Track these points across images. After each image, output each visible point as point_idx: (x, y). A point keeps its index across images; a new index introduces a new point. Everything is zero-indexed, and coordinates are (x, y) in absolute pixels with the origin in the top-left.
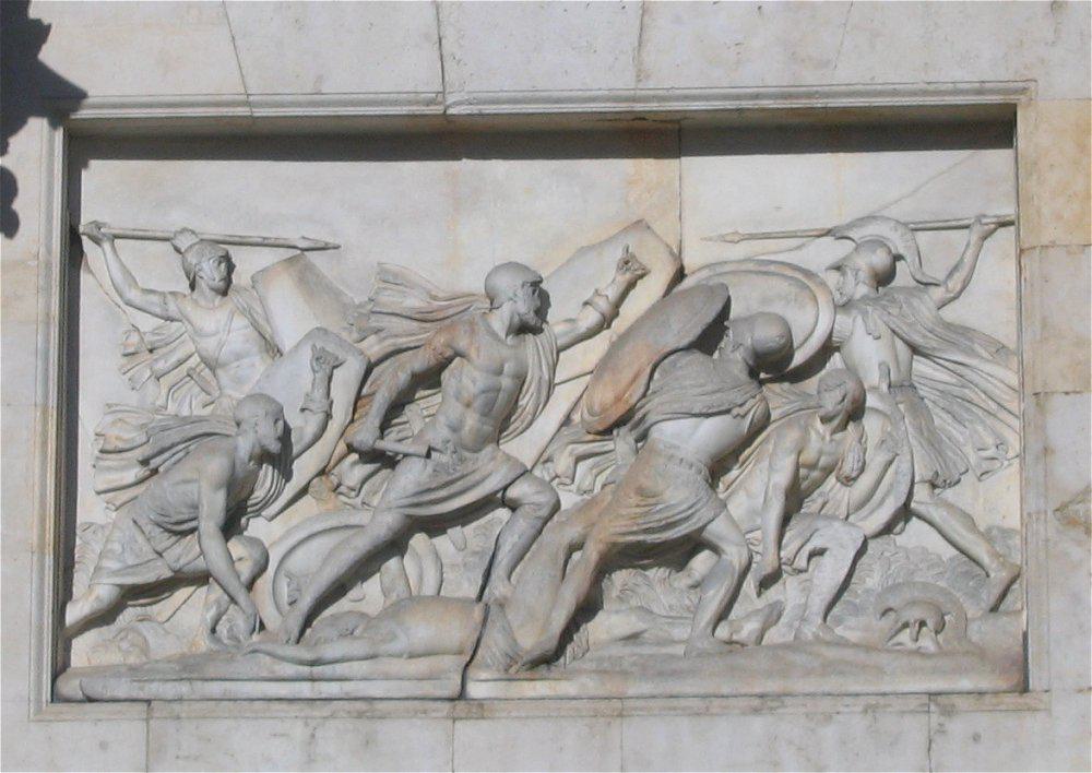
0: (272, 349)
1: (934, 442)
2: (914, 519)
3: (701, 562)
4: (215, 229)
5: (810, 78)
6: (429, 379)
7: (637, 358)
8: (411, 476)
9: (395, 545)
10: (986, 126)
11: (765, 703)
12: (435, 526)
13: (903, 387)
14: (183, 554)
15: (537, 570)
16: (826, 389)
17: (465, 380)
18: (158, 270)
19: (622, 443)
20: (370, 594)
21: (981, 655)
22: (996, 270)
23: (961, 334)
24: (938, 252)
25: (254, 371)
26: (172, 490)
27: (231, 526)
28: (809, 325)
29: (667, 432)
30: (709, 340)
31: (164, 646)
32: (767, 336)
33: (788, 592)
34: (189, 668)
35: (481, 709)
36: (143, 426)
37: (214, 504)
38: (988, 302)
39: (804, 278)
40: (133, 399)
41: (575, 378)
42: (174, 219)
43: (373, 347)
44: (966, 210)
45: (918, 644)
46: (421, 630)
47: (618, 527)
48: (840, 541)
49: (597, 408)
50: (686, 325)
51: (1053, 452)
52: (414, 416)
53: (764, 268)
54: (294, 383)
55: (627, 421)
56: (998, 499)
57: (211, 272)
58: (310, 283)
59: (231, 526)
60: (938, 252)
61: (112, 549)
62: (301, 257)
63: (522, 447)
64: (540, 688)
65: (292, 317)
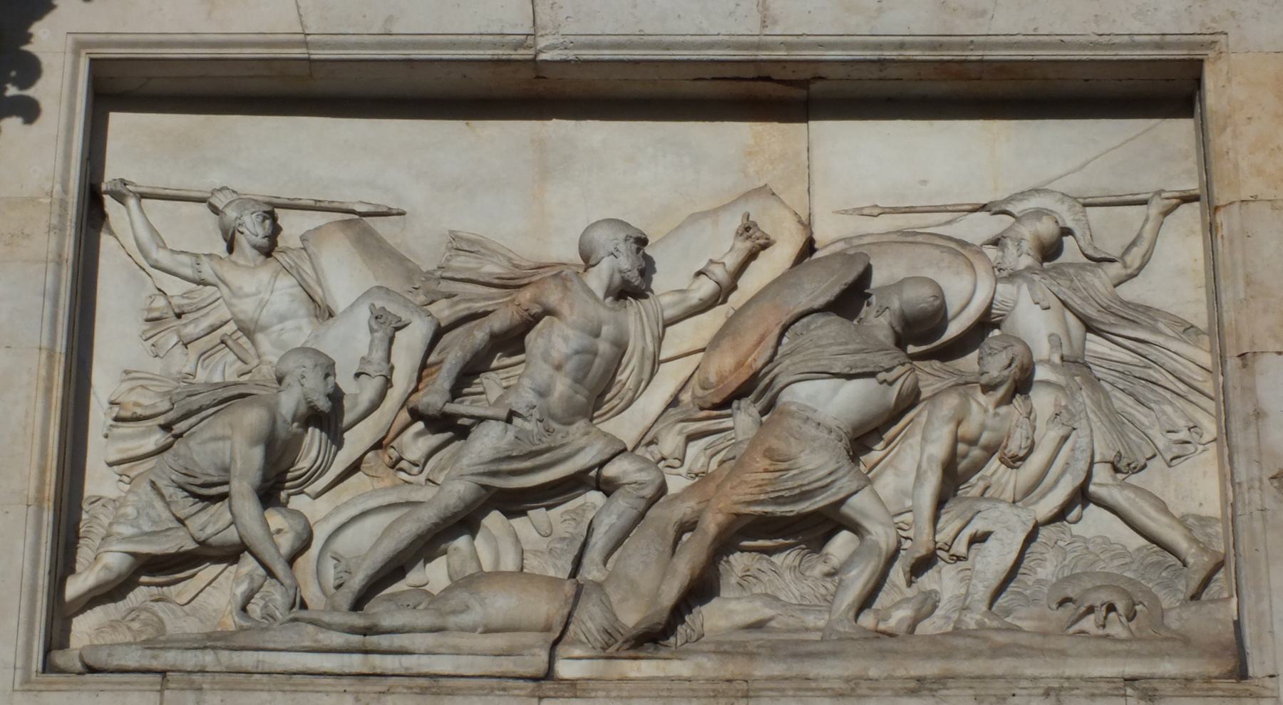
0: (323, 312)
2: (1092, 506)
3: (841, 544)
5: (963, 26)
6: (511, 341)
8: (488, 442)
9: (464, 522)
12: (514, 503)
13: (1075, 363)
14: (212, 524)
16: (992, 361)
17: (555, 342)
18: (192, 231)
19: (744, 418)
20: (434, 574)
21: (1184, 643)
22: (1181, 246)
23: (1142, 314)
25: (300, 330)
27: (269, 494)
28: (965, 295)
29: (802, 394)
30: (850, 300)
32: (919, 298)
36: (165, 394)
38: (1173, 274)
39: (960, 249)
40: (156, 367)
41: (687, 353)
43: (444, 311)
44: (1144, 184)
45: (1108, 630)
47: (742, 495)
49: (713, 378)
50: (821, 287)
51: (1265, 415)
52: (491, 384)
53: (907, 238)
54: (350, 342)
55: (753, 388)
56: (1196, 487)
57: (253, 229)
59: (269, 494)
61: (125, 512)
62: (360, 223)
63: (626, 427)
64: (645, 668)
65: (345, 276)
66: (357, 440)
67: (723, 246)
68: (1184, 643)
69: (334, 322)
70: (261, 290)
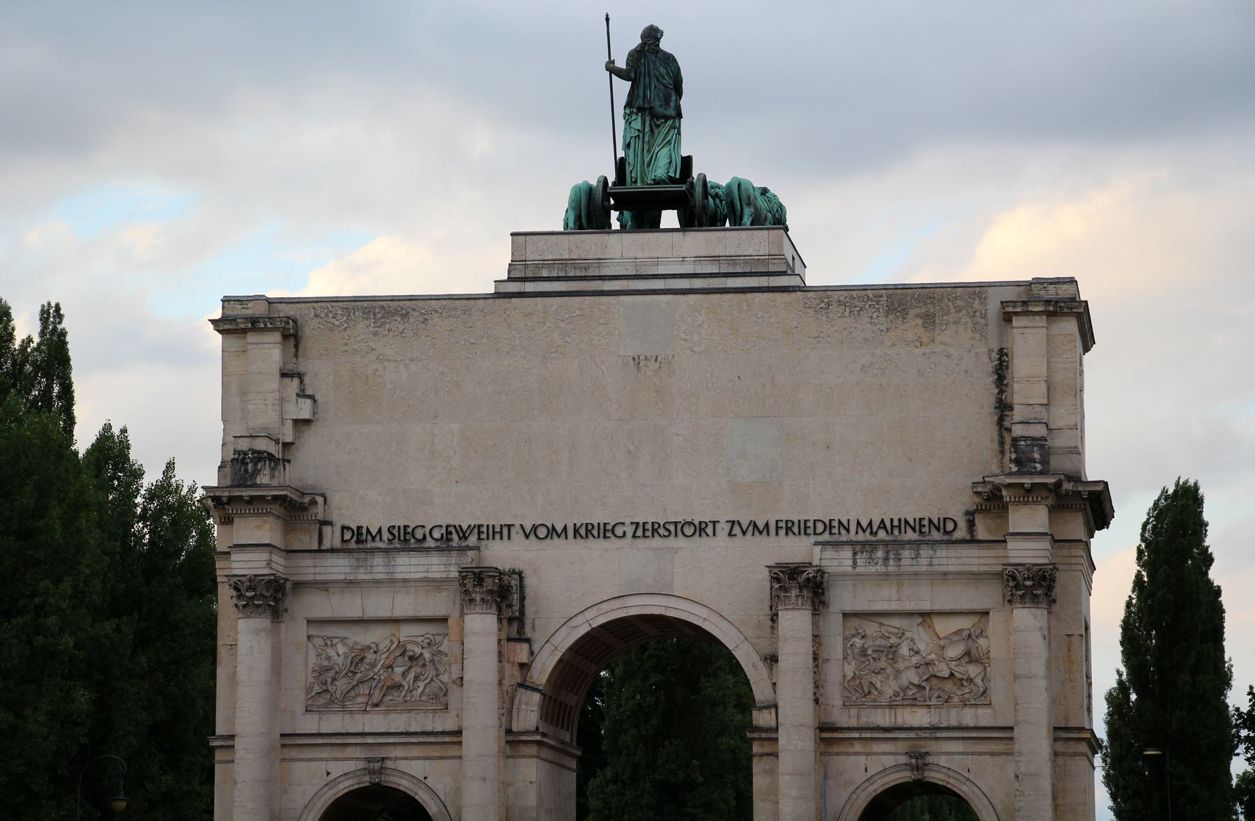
1: (436, 669)
7: (392, 657)
8: (358, 676)
10: (444, 620)
15: (377, 691)
20: (352, 694)
24: (438, 639)
26: (322, 678)
28: (418, 650)
30: (403, 654)
34: (325, 706)
39: (417, 643)
46: (360, 700)
48: (422, 685)
50: (398, 652)
53: (411, 642)
54: (340, 661)
55: (391, 667)
58: (344, 644)
60: (438, 639)
62: (343, 640)
63: (376, 670)
65: (341, 649)
67: (387, 642)
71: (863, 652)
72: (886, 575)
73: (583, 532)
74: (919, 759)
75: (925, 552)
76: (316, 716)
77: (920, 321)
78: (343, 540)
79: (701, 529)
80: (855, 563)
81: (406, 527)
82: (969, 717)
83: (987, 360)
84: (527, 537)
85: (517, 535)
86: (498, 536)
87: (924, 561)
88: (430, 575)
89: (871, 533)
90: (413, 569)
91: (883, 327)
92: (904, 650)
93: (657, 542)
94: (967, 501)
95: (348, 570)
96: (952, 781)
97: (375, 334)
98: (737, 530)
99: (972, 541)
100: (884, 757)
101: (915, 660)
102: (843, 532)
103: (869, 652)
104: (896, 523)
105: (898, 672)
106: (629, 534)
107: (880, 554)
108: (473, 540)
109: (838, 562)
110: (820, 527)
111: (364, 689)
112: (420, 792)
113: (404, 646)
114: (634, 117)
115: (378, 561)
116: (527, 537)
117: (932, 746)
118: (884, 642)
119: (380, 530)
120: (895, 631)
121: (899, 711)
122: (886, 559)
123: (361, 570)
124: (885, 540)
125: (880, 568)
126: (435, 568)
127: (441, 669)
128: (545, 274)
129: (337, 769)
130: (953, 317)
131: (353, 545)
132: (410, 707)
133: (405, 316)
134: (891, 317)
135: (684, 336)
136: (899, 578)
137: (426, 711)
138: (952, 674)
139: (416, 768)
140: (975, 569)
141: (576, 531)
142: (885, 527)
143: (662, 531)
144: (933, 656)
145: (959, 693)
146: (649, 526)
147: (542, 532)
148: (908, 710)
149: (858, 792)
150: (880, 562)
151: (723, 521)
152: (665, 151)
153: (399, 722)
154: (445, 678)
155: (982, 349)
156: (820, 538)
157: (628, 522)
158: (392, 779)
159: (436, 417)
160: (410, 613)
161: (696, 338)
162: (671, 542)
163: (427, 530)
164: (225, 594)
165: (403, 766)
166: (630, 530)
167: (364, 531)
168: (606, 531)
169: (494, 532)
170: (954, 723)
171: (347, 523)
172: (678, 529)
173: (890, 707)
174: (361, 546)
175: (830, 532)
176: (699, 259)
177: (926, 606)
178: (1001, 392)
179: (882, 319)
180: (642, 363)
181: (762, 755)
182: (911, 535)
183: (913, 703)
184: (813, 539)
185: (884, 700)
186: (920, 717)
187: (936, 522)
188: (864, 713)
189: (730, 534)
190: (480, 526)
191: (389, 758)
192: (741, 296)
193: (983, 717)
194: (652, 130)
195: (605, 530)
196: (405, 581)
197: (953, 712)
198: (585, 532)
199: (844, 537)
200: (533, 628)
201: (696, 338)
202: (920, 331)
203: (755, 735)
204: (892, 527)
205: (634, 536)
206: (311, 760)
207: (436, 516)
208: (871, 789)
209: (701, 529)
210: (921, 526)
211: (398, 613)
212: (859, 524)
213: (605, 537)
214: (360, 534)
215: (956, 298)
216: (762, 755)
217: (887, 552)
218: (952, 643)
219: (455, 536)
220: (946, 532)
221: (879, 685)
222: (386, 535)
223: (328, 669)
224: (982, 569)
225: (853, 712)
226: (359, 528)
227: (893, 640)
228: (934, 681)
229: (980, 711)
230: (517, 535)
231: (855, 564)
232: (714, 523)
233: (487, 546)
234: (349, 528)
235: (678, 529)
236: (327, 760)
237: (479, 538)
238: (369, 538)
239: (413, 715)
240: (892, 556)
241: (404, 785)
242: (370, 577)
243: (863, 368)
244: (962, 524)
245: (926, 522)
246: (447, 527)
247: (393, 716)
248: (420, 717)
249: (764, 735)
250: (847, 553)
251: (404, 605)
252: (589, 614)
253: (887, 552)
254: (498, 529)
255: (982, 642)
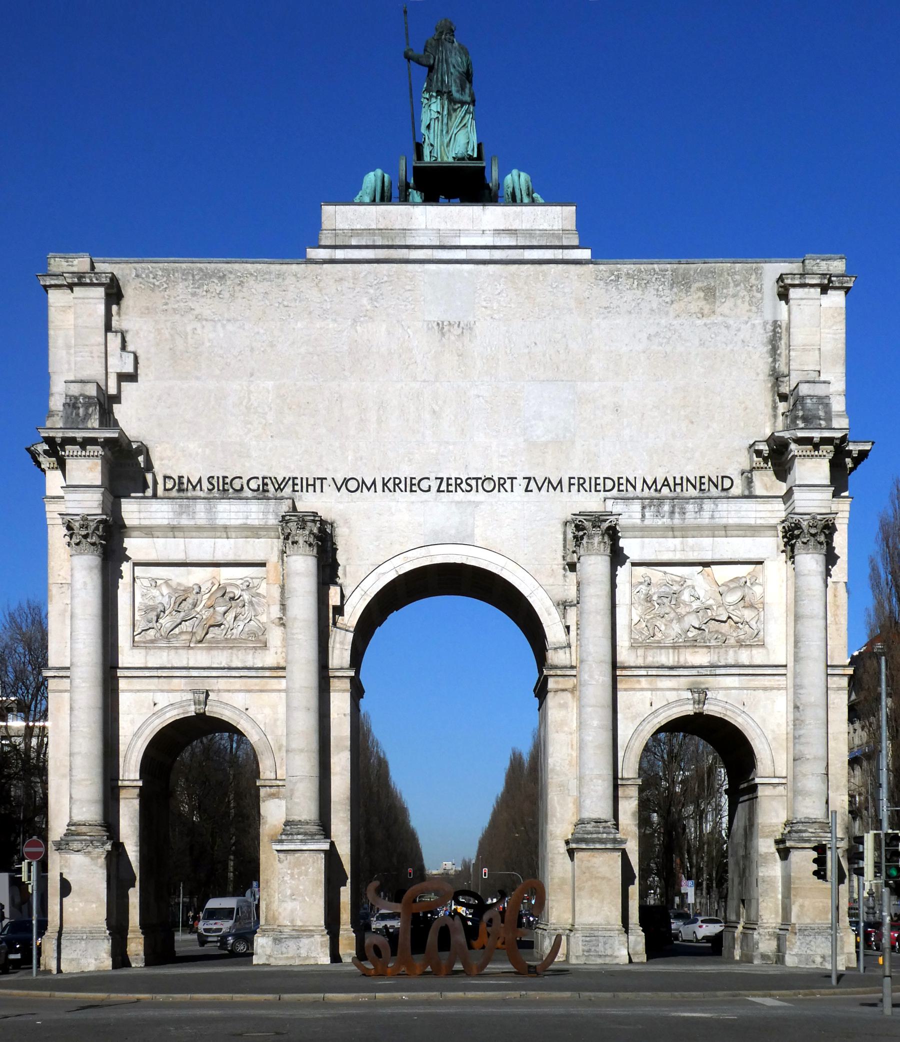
1: (255, 610)
3: (222, 627)
4: (154, 577)
5: (238, 558)
6: (185, 600)
7: (213, 598)
8: (182, 614)
9: (180, 624)
10: (263, 565)
11: (231, 648)
13: (251, 603)
14: (150, 625)
18: (146, 583)
19: (212, 609)
20: (177, 631)
21: (260, 641)
23: (258, 595)
25: (160, 597)
27: (157, 621)
28: (237, 593)
29: (217, 609)
31: (148, 638)
32: (232, 595)
33: (234, 631)
34: (152, 641)
35: (192, 648)
37: (155, 618)
39: (237, 586)
42: (149, 575)
43: (177, 595)
44: (260, 576)
46: (184, 637)
47: (211, 622)
48: (242, 624)
50: (221, 594)
53: (231, 585)
57: (154, 584)
59: (157, 621)
61: (141, 625)
62: (167, 582)
63: (198, 609)
64: (200, 645)
65: (165, 590)
66: (167, 613)
67: (209, 585)
68: (260, 641)
69: (163, 597)
70: (155, 592)
71: (648, 599)
72: (672, 529)
73: (390, 485)
74: (701, 694)
75: (708, 505)
76: (143, 651)
77: (702, 294)
78: (165, 490)
79: (500, 484)
80: (643, 516)
81: (224, 478)
82: (744, 656)
83: (762, 331)
84: (339, 490)
85: (329, 488)
86: (311, 488)
87: (706, 514)
88: (249, 522)
89: (656, 490)
90: (233, 515)
91: (668, 299)
92: (686, 596)
93: (460, 495)
94: (744, 461)
95: (171, 515)
96: (729, 713)
97: (194, 294)
98: (532, 485)
99: (751, 496)
100: (668, 693)
101: (696, 605)
102: (630, 488)
103: (655, 598)
104: (678, 481)
105: (680, 618)
106: (434, 489)
107: (666, 508)
108: (288, 490)
109: (629, 514)
110: (609, 484)
111: (185, 626)
112: (242, 722)
113: (225, 588)
114: (434, 100)
115: (200, 506)
116: (339, 490)
117: (711, 681)
118: (668, 590)
119: (200, 481)
120: (678, 579)
121: (682, 650)
122: (672, 512)
123: (184, 516)
124: (671, 496)
125: (666, 521)
126: (254, 516)
127: (260, 610)
128: (354, 242)
129: (164, 700)
130: (731, 290)
131: (174, 493)
132: (230, 644)
133: (222, 278)
134: (675, 290)
135: (484, 304)
136: (683, 531)
137: (246, 648)
138: (729, 617)
139: (239, 700)
140: (752, 522)
141: (385, 484)
142: (668, 485)
143: (464, 486)
144: (711, 602)
145: (735, 634)
146: (452, 482)
147: (352, 485)
148: (690, 650)
149: (644, 724)
150: (667, 515)
151: (520, 478)
152: (463, 132)
153: (221, 658)
154: (263, 618)
155: (758, 321)
156: (608, 494)
157: (432, 477)
158: (215, 709)
159: (252, 375)
160: (231, 558)
161: (495, 306)
162: (472, 496)
163: (245, 481)
164: (57, 535)
165: (225, 697)
166: (435, 485)
167: (185, 480)
168: (413, 485)
169: (308, 485)
170: (731, 661)
171: (169, 473)
172: (480, 483)
173: (674, 647)
174: (181, 494)
175: (619, 486)
176: (498, 232)
177: (708, 557)
178: (775, 361)
179: (667, 292)
180: (446, 329)
181: (556, 691)
182: (692, 492)
183: (694, 644)
184: (602, 494)
185: (668, 642)
186: (701, 658)
187: (715, 480)
188: (650, 653)
189: (526, 490)
190: (294, 478)
191: (213, 691)
192: (537, 266)
193: (758, 656)
194: (449, 114)
195: (412, 485)
196: (226, 528)
197: (731, 652)
198: (392, 485)
199: (631, 492)
200: (345, 574)
201: (495, 306)
202: (702, 303)
203: (551, 673)
204: (675, 484)
205: (439, 491)
206: (139, 691)
207: (252, 467)
208: (656, 721)
209: (500, 484)
210: (702, 484)
211: (220, 557)
212: (644, 481)
213: (411, 491)
214: (181, 483)
215: (735, 273)
216: (556, 691)
217: (673, 507)
218: (730, 590)
219: (270, 487)
220: (723, 490)
221: (663, 628)
222: (205, 485)
223: (153, 609)
224: (759, 522)
225: (640, 652)
226: (180, 477)
227: (675, 588)
228: (713, 625)
229: (755, 651)
230: (329, 488)
231: (643, 516)
232: (512, 479)
233: (300, 497)
234: (170, 478)
235: (480, 483)
236: (154, 691)
237: (294, 491)
238: (190, 487)
239: (235, 651)
240: (677, 510)
241: (227, 715)
242: (192, 522)
243: (649, 338)
244: (739, 482)
245: (705, 480)
246: (264, 478)
247: (215, 653)
248: (241, 654)
249: (559, 672)
250: (636, 506)
251: (225, 549)
252: (397, 561)
253: (673, 507)
254: (311, 482)
255: (758, 590)
